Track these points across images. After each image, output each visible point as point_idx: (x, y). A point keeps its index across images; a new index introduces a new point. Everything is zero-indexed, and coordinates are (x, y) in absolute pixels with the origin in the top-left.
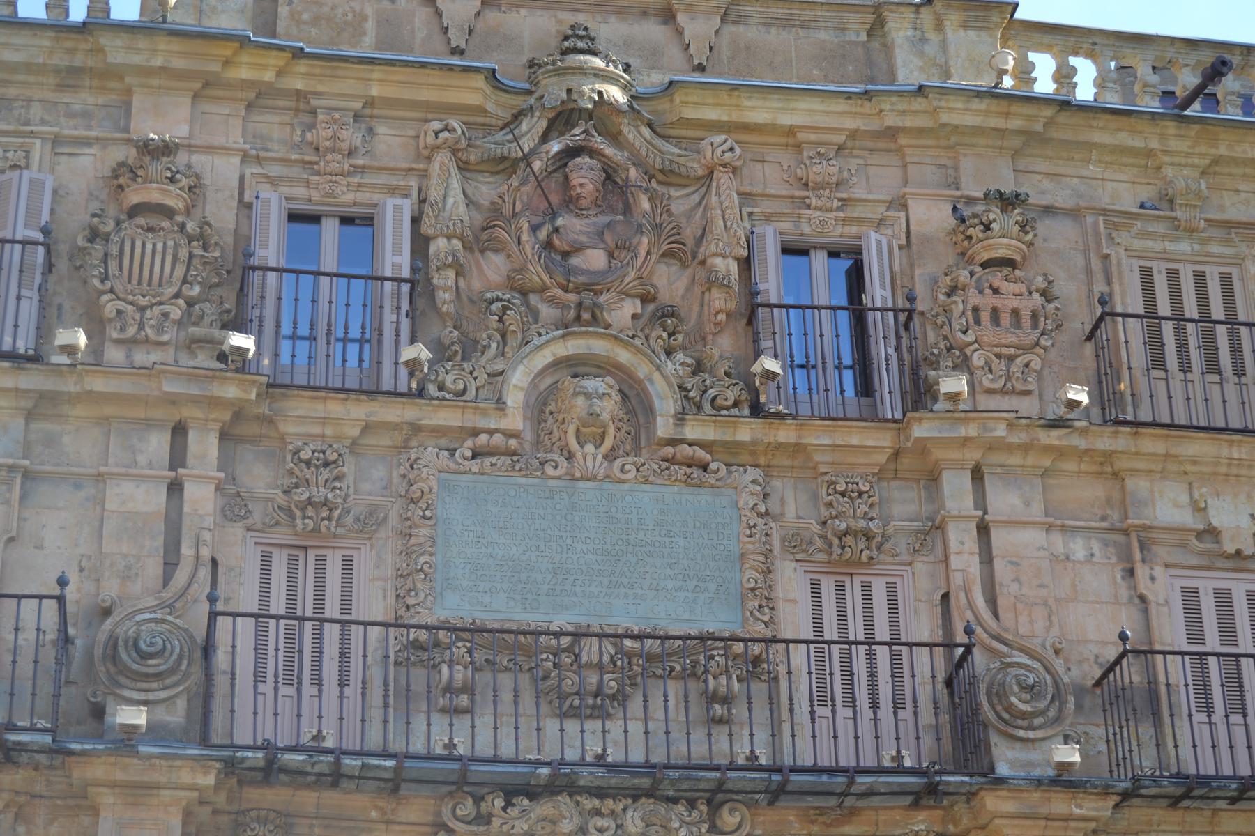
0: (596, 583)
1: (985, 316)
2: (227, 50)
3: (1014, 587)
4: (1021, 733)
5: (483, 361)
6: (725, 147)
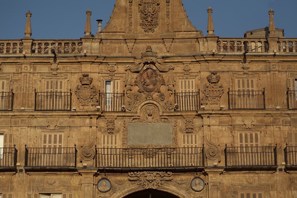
3: (213, 135)
4: (212, 159)
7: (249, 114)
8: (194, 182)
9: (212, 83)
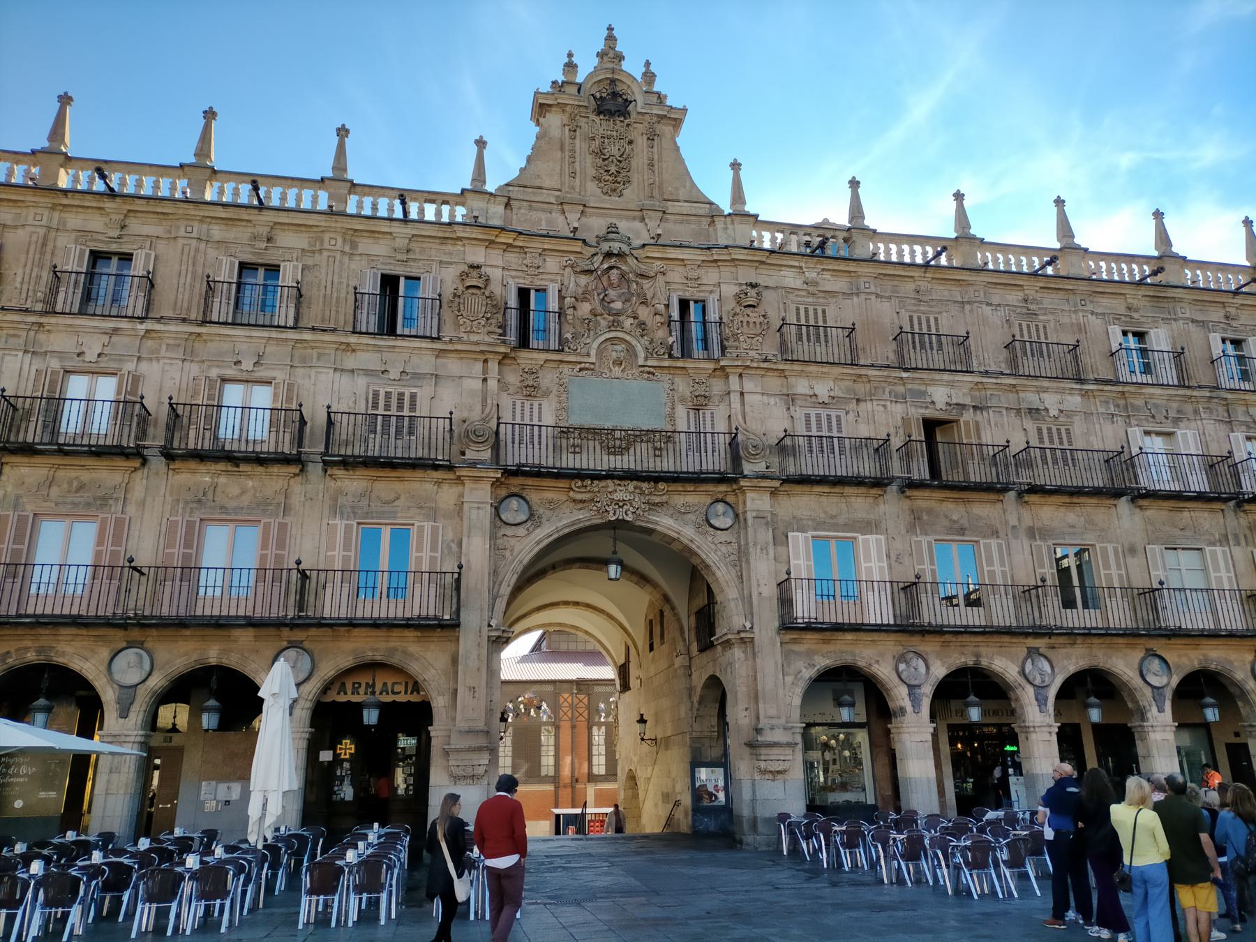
1: (745, 324)
2: (496, 232)
7: (825, 373)
8: (712, 510)
9: (745, 307)
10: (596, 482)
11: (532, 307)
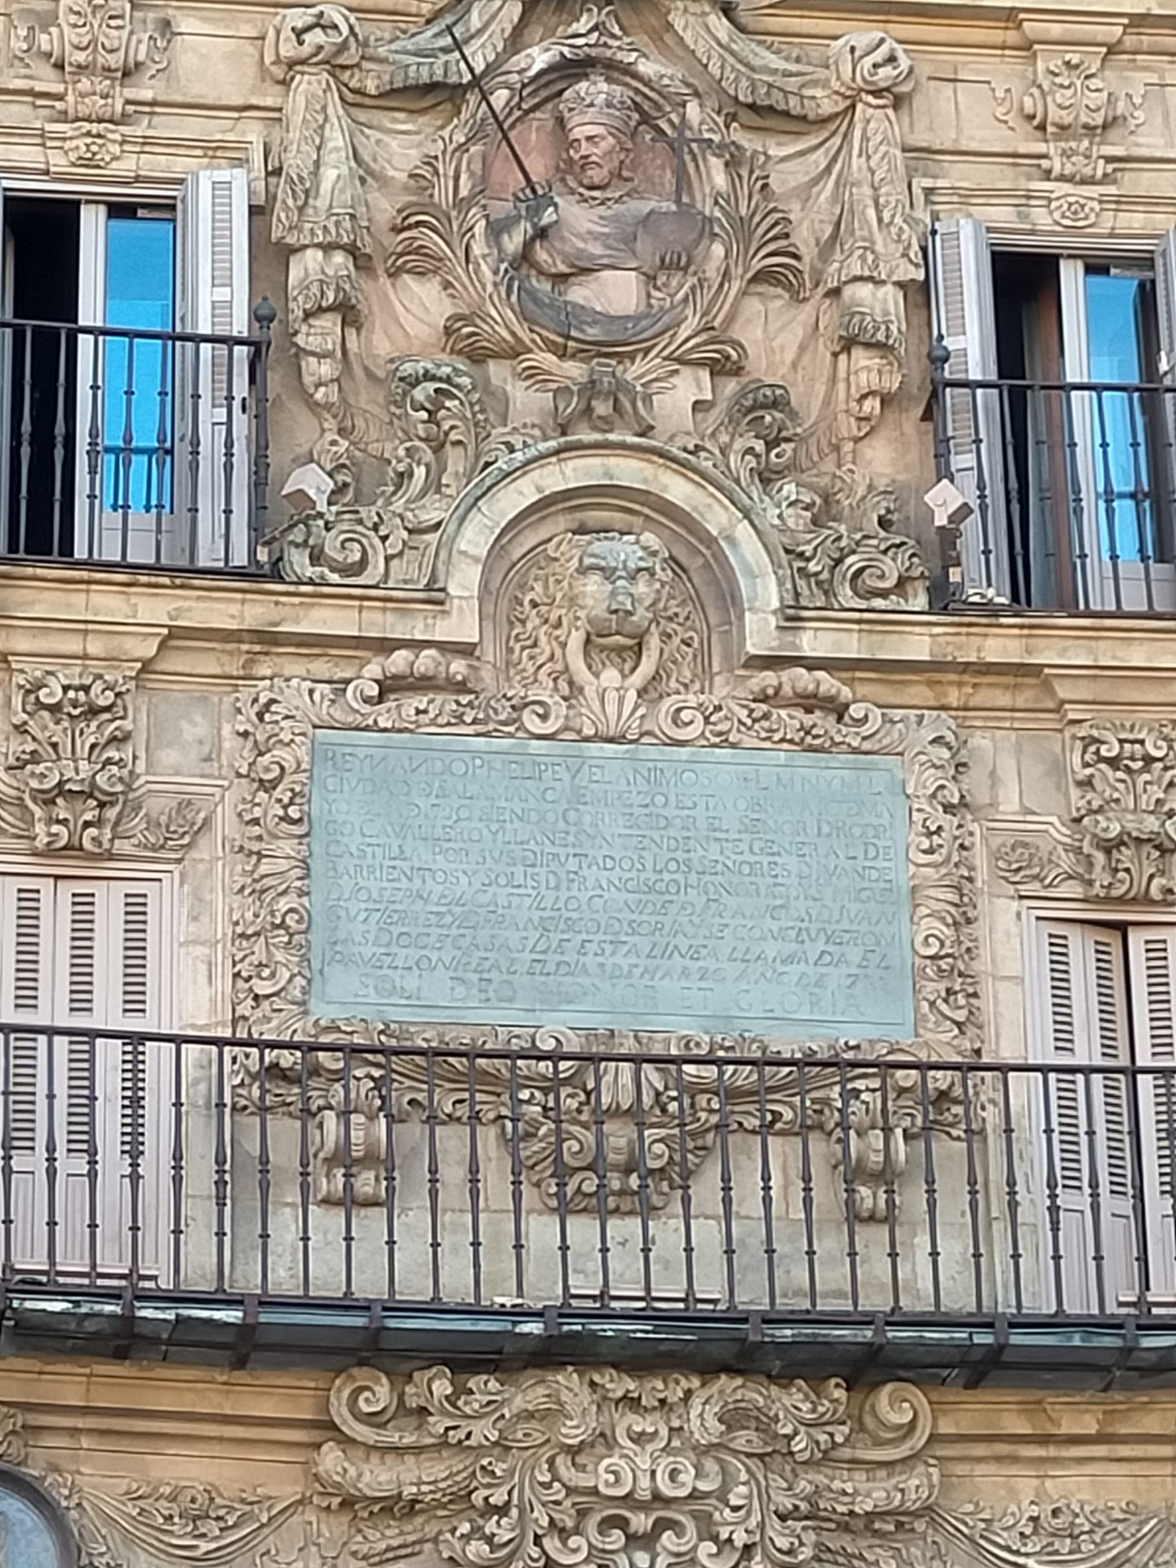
0: (625, 948)
5: (398, 505)
6: (879, 55)
10: (484, 1386)
11: (90, 310)
